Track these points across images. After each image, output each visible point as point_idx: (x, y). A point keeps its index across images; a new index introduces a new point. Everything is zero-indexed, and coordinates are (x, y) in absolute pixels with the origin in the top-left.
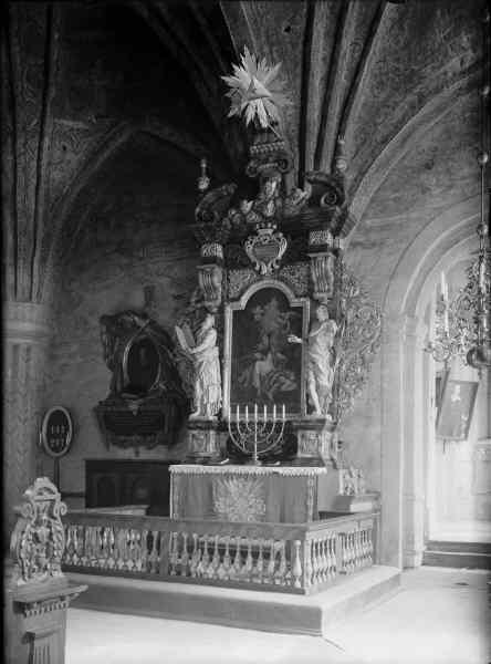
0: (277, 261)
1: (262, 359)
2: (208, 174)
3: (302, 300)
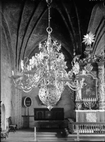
0: (91, 71)
1: (87, 89)
2: (75, 52)
3: (96, 78)
